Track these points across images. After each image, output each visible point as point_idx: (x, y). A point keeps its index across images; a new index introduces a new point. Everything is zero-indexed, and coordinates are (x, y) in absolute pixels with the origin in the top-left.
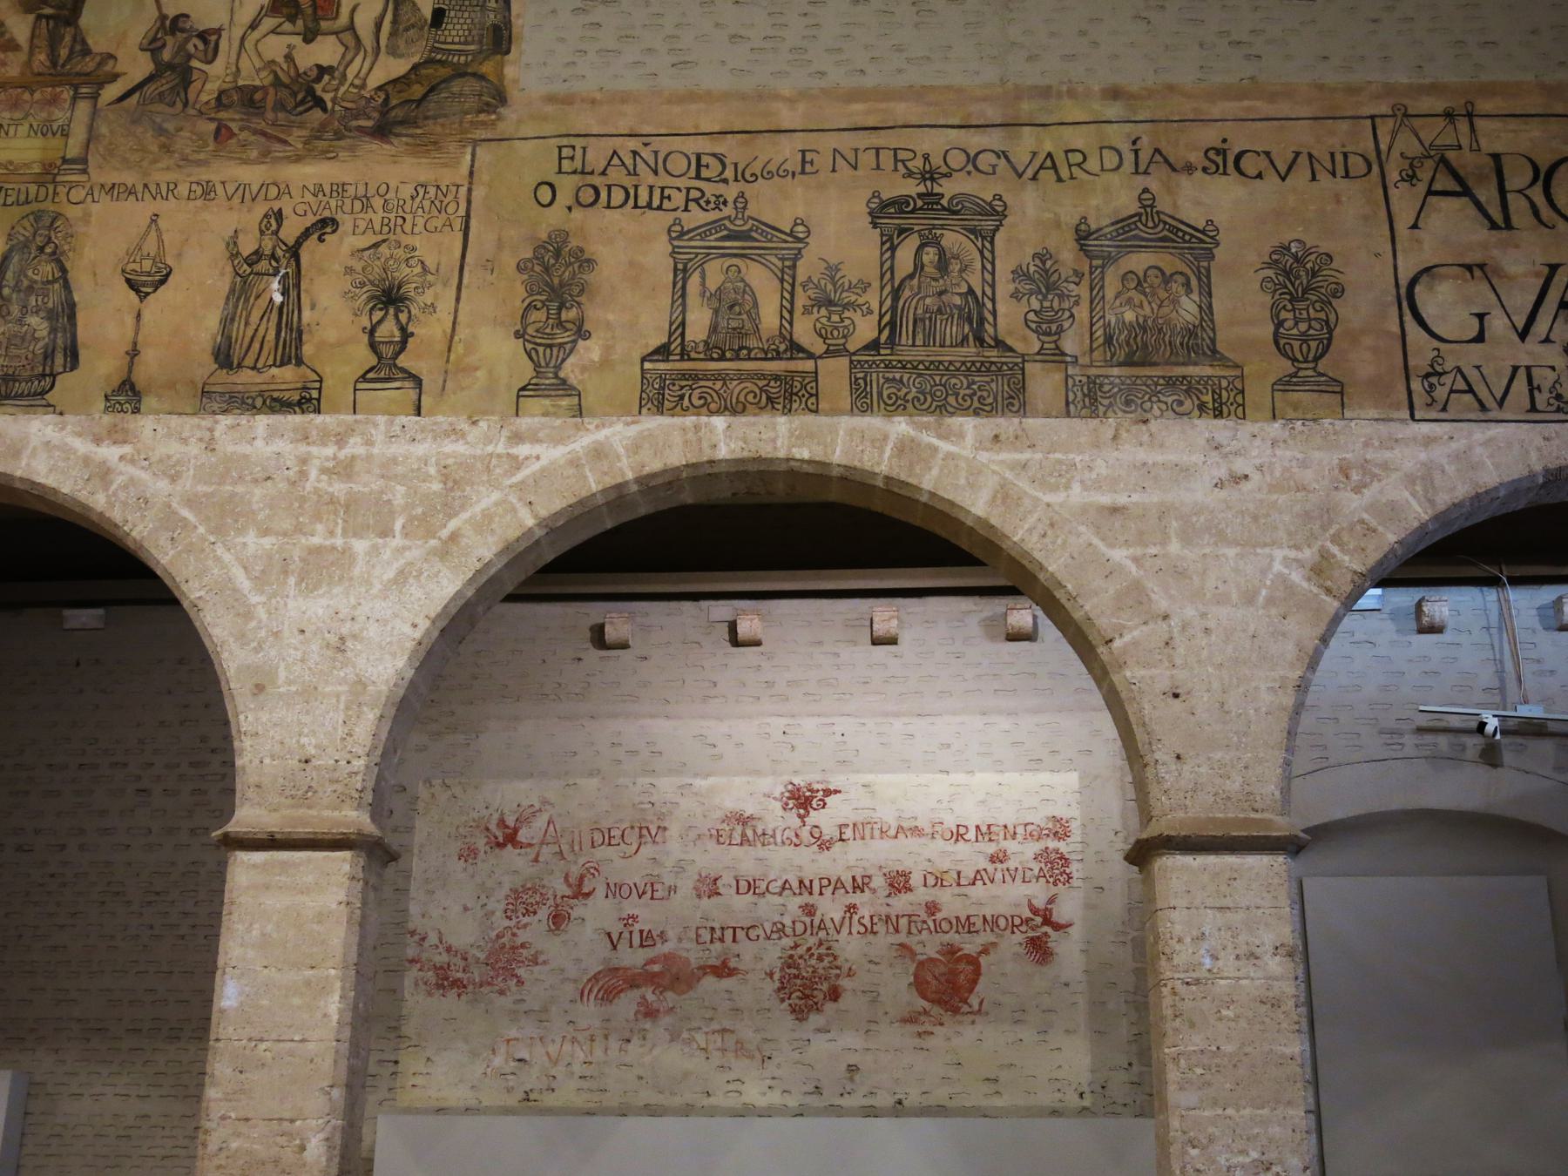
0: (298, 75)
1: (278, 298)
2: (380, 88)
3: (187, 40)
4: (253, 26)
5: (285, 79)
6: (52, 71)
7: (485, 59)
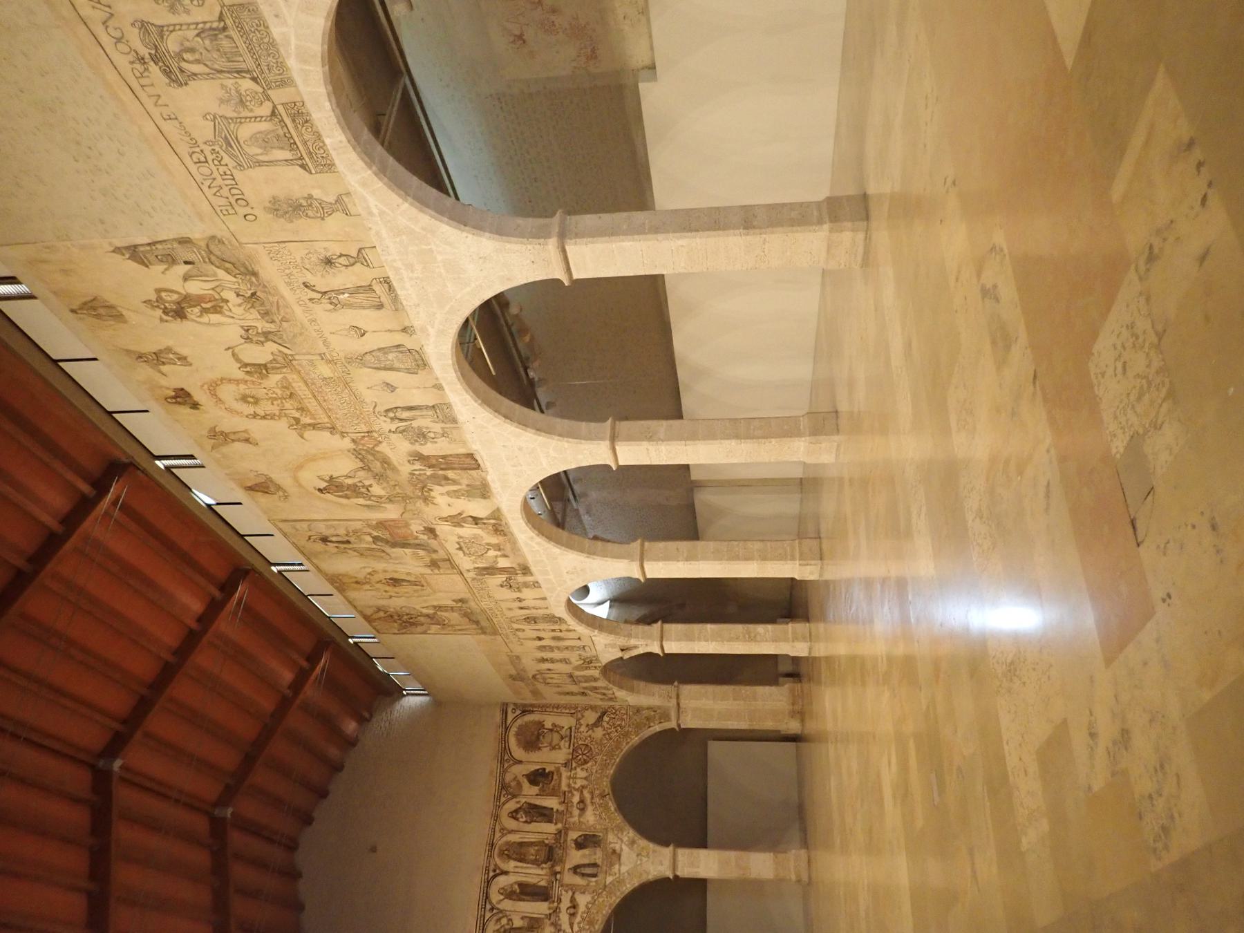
1: (346, 295)
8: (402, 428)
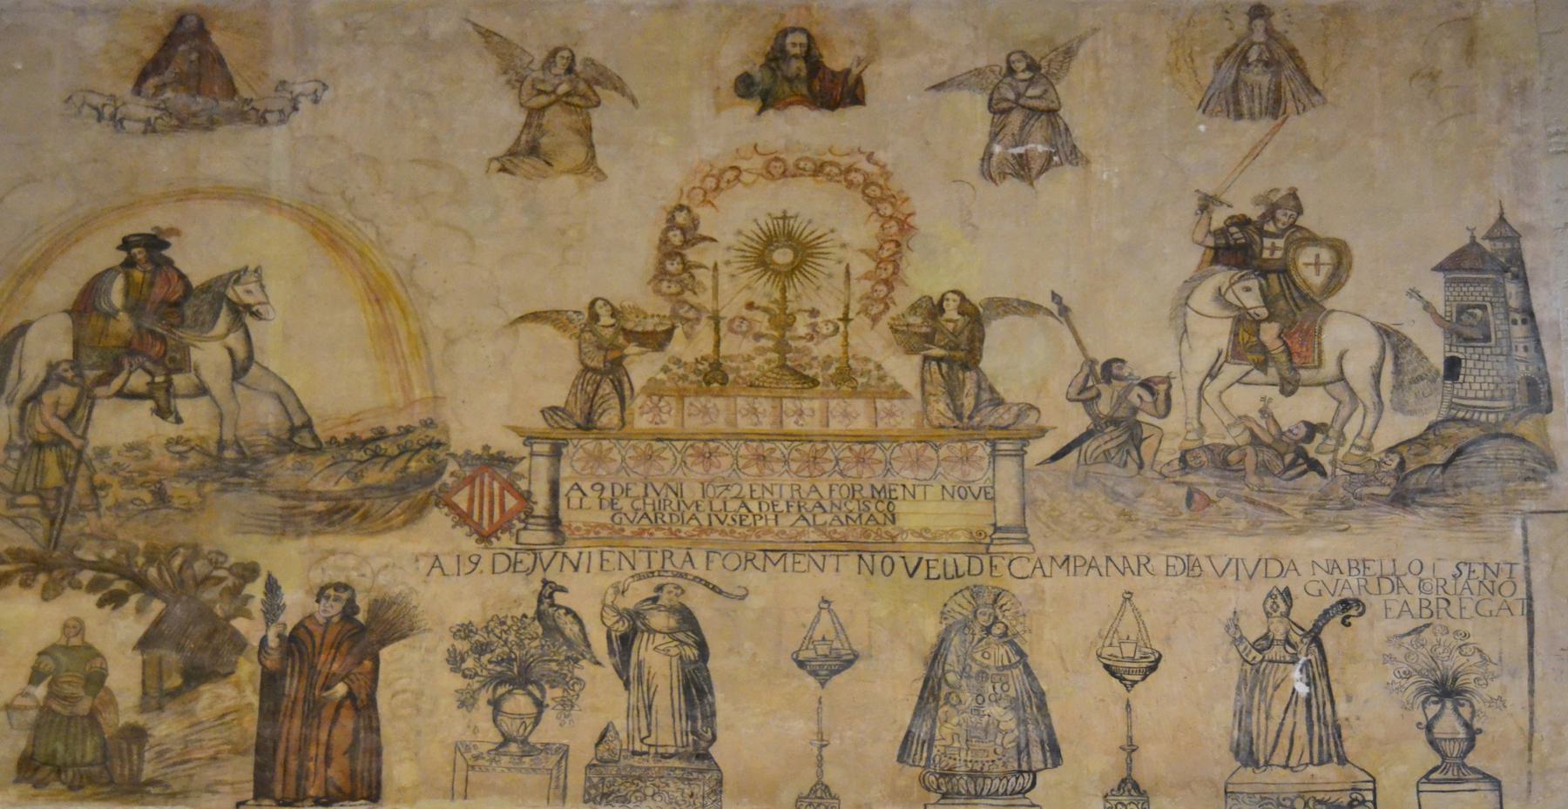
0: (1283, 434)
1: (1302, 689)
2: (1391, 450)
3: (1128, 389)
4: (1212, 374)
5: (1267, 439)
6: (957, 423)
7: (1521, 418)
8: (571, 629)
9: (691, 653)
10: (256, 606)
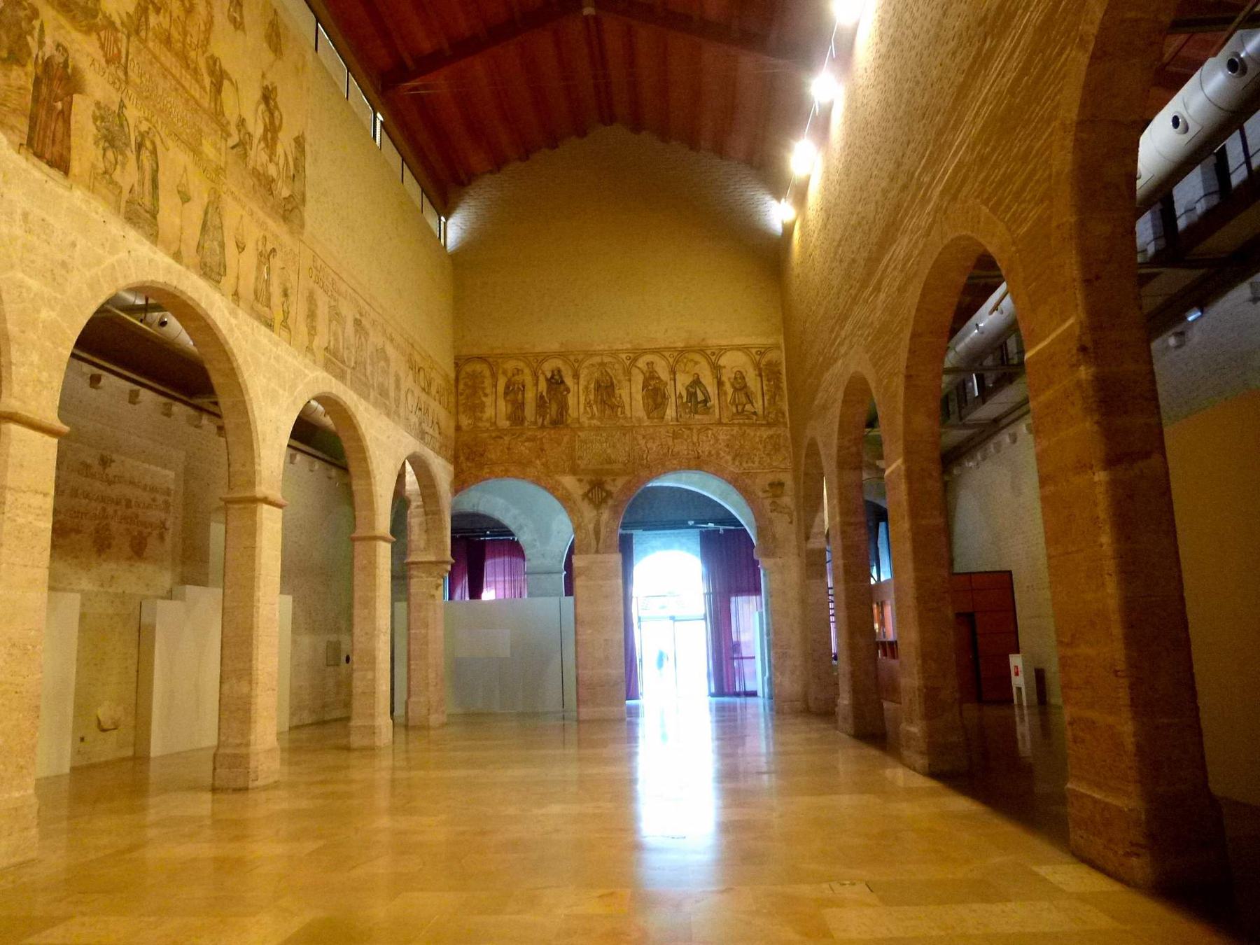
8: (126, 129)
9: (155, 166)
10: (36, 33)
